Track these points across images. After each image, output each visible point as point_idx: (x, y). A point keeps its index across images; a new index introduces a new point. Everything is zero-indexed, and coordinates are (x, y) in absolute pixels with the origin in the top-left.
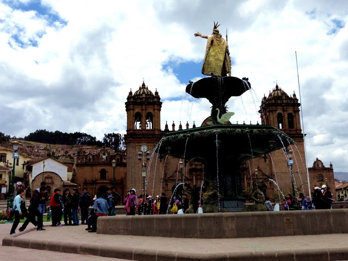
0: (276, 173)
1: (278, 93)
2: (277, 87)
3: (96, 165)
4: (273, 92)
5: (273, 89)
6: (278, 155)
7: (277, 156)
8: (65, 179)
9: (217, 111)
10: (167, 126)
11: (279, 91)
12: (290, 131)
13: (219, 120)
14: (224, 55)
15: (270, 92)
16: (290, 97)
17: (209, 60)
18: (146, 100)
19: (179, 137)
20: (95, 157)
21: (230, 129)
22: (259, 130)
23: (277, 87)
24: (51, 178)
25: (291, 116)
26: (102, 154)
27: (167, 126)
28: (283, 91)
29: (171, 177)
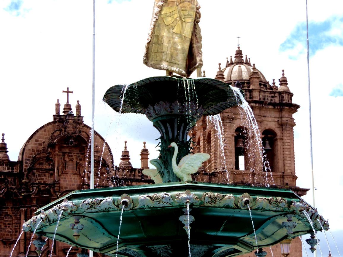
1: (240, 72)
2: (239, 54)
4: (227, 66)
5: (229, 60)
9: (174, 148)
11: (243, 67)
13: (176, 168)
14: (192, 26)
15: (220, 68)
16: (271, 84)
17: (160, 34)
19: (102, 202)
21: (213, 194)
22: (267, 198)
23: (239, 54)
25: (269, 137)
28: (254, 68)
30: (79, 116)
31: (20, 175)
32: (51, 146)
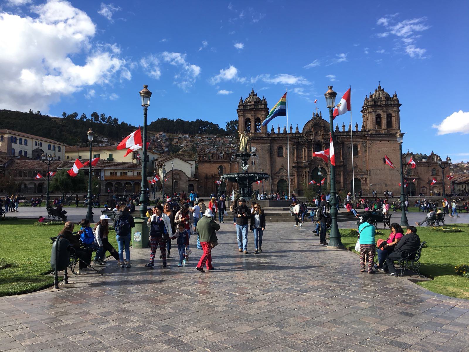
0: (372, 169)
2: (380, 87)
3: (215, 162)
6: (374, 153)
7: (373, 154)
8: (189, 175)
10: (273, 129)
11: (380, 92)
12: (387, 130)
18: (254, 107)
20: (214, 155)
24: (179, 174)
25: (389, 116)
26: (219, 153)
27: (273, 129)
29: (277, 173)
30: (321, 117)
31: (303, 137)
32: (312, 127)
